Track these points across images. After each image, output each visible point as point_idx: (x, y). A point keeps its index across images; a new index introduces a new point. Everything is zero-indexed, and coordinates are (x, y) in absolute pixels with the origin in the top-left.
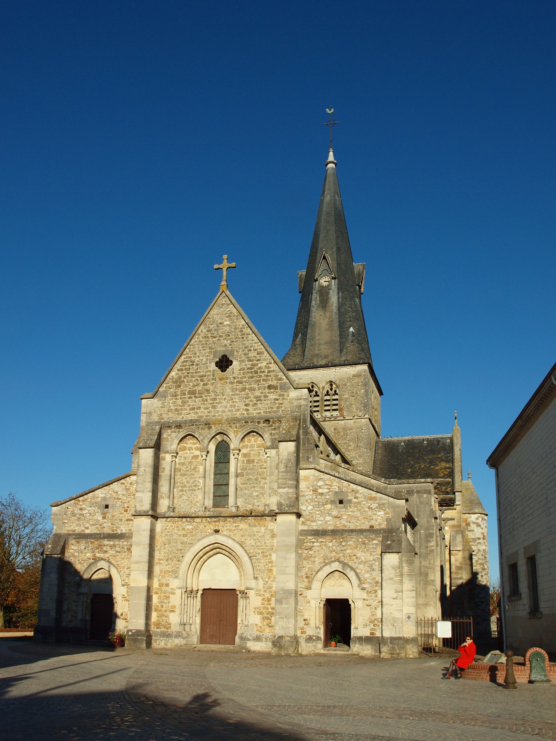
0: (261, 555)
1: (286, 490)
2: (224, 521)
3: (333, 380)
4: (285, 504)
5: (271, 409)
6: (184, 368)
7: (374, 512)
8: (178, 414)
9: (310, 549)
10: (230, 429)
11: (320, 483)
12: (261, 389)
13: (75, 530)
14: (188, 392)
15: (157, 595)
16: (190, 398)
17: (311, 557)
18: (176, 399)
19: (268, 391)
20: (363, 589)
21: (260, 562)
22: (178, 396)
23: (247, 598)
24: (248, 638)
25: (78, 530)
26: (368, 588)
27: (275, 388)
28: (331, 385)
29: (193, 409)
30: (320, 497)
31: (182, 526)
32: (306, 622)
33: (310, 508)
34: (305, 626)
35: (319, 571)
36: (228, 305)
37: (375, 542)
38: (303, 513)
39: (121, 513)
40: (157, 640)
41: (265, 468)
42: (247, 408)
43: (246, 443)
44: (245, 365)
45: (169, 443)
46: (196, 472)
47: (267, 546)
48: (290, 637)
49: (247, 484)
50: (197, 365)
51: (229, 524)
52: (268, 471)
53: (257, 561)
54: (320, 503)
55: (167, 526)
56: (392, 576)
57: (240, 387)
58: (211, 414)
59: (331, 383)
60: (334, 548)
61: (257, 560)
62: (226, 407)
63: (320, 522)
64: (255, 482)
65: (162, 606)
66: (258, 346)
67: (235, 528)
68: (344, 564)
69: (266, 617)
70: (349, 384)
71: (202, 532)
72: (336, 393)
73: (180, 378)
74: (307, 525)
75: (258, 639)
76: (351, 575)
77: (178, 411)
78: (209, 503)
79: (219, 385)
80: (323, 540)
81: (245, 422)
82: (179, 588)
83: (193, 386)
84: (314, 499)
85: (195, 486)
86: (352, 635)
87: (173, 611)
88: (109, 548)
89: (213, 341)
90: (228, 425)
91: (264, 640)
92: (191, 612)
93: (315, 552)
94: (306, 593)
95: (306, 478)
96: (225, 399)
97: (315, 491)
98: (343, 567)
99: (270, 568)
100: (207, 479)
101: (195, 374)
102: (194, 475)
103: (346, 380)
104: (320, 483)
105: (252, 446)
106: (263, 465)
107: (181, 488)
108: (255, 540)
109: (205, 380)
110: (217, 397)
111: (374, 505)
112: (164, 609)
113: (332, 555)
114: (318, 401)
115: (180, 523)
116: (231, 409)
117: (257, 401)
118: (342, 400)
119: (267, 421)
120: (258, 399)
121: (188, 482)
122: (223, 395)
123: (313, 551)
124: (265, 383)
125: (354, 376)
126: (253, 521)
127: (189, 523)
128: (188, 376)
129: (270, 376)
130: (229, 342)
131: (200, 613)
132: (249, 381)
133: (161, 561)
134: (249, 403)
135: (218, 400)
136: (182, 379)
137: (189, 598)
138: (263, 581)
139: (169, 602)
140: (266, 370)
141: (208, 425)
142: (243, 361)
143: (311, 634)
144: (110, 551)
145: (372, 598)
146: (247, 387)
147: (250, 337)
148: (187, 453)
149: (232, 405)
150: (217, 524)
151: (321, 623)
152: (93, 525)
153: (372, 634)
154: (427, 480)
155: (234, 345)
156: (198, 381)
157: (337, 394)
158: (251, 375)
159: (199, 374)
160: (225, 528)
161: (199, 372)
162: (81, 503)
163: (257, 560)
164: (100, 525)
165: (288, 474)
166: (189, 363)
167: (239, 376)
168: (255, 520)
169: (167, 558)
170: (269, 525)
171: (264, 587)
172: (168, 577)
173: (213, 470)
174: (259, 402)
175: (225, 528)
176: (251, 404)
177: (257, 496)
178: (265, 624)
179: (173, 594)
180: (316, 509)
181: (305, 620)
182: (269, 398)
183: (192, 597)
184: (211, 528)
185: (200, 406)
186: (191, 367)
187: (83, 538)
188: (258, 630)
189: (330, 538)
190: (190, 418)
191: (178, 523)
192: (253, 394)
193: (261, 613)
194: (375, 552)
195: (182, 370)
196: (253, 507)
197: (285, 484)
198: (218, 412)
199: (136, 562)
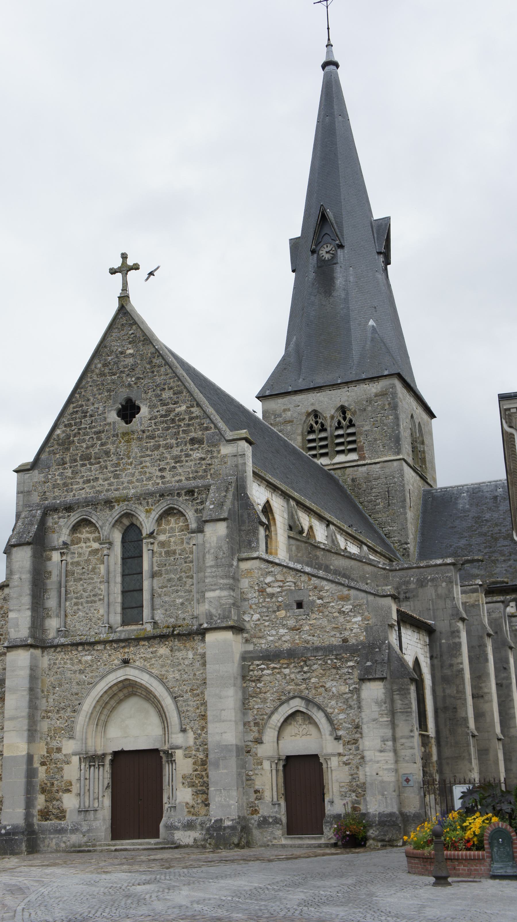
0: (190, 693)
1: (217, 593)
2: (136, 646)
3: (346, 404)
4: (217, 615)
5: (195, 474)
6: (73, 422)
7: (348, 618)
8: (67, 491)
9: (259, 680)
10: (140, 507)
11: (269, 579)
12: (181, 445)
14: (80, 457)
15: (45, 767)
16: (83, 465)
17: (260, 693)
18: (64, 469)
19: (190, 447)
20: (338, 738)
21: (188, 705)
22: (66, 463)
23: (173, 762)
24: (175, 826)
26: (345, 737)
27: (200, 442)
28: (344, 413)
29: (88, 481)
30: (269, 600)
31: (77, 658)
32: (258, 794)
33: (256, 617)
34: (256, 802)
35: (272, 713)
37: (351, 664)
38: (248, 626)
40: (45, 838)
41: (192, 562)
42: (163, 474)
43: (164, 526)
44: (157, 412)
45: (55, 536)
46: (95, 574)
47: (198, 679)
48: (232, 820)
49: (167, 587)
50: (91, 416)
51: (142, 650)
52: (195, 566)
53: (184, 704)
54: (270, 609)
55: (57, 659)
56: (376, 715)
57: (152, 444)
58: (112, 488)
59: (343, 410)
60: (293, 676)
61: (184, 701)
62: (133, 475)
63: (271, 638)
64: (178, 582)
65: (52, 784)
66: (174, 381)
67: (152, 655)
68: (308, 701)
69: (199, 791)
70: (370, 408)
71: (105, 665)
72: (351, 424)
73: (68, 437)
74: (253, 642)
75: (189, 826)
76: (319, 717)
77: (67, 486)
78: (116, 618)
80: (276, 666)
81: (160, 496)
82: (75, 754)
83: (87, 448)
84: (261, 603)
85: (94, 595)
86: (327, 812)
87: (68, 791)
89: (112, 380)
90: (136, 502)
91: (199, 827)
92: (96, 791)
93: (265, 684)
94: (256, 748)
95: (249, 571)
96: (131, 463)
97: (262, 591)
98: (307, 705)
99: (203, 713)
100: (112, 584)
101: (88, 430)
102: (92, 579)
103: (365, 403)
104: (269, 579)
105: (172, 530)
106: (188, 557)
107: (74, 600)
108: (179, 671)
109: (103, 437)
110: (121, 462)
111: (347, 607)
112: (55, 788)
113: (290, 687)
114: (325, 439)
115: (74, 652)
116: (140, 477)
117: (176, 462)
118: (361, 434)
120: (177, 460)
121: (85, 590)
122: (129, 458)
123: (263, 683)
124: (185, 435)
125: (376, 395)
126: (177, 643)
127: (87, 653)
128: (79, 433)
129: (193, 425)
130: (133, 379)
131: (110, 790)
132: (163, 434)
133: (50, 714)
134: (166, 467)
135: (122, 465)
136: (71, 438)
137: (92, 768)
138: (194, 733)
139: (62, 777)
140: (187, 417)
141: (109, 503)
142: (155, 406)
143: (266, 814)
145: (351, 751)
146: (161, 443)
147: (163, 369)
148: (82, 548)
149: (141, 472)
150: (127, 650)
151: (281, 796)
153: (354, 809)
154: (445, 560)
155: (142, 383)
156: (93, 440)
158: (166, 425)
159: (94, 429)
160: (138, 656)
161: (94, 427)
163: (184, 701)
165: (220, 569)
166: (80, 415)
167: (150, 428)
168: (179, 640)
169: (57, 708)
170: (199, 648)
171: (195, 743)
172: (59, 737)
173: (119, 569)
174: (178, 464)
175: (138, 656)
176: (168, 469)
177: (182, 604)
178: (199, 801)
179: (68, 763)
180: (264, 618)
181: (256, 792)
182: (192, 458)
183: (97, 766)
185: (97, 476)
186: (83, 421)
188: (189, 812)
189: (286, 661)
190: (83, 496)
191: (71, 653)
192: (169, 453)
193: (192, 785)
194: (352, 679)
195: (70, 425)
196: (177, 620)
197: (215, 585)
198: (123, 483)
199: (12, 719)
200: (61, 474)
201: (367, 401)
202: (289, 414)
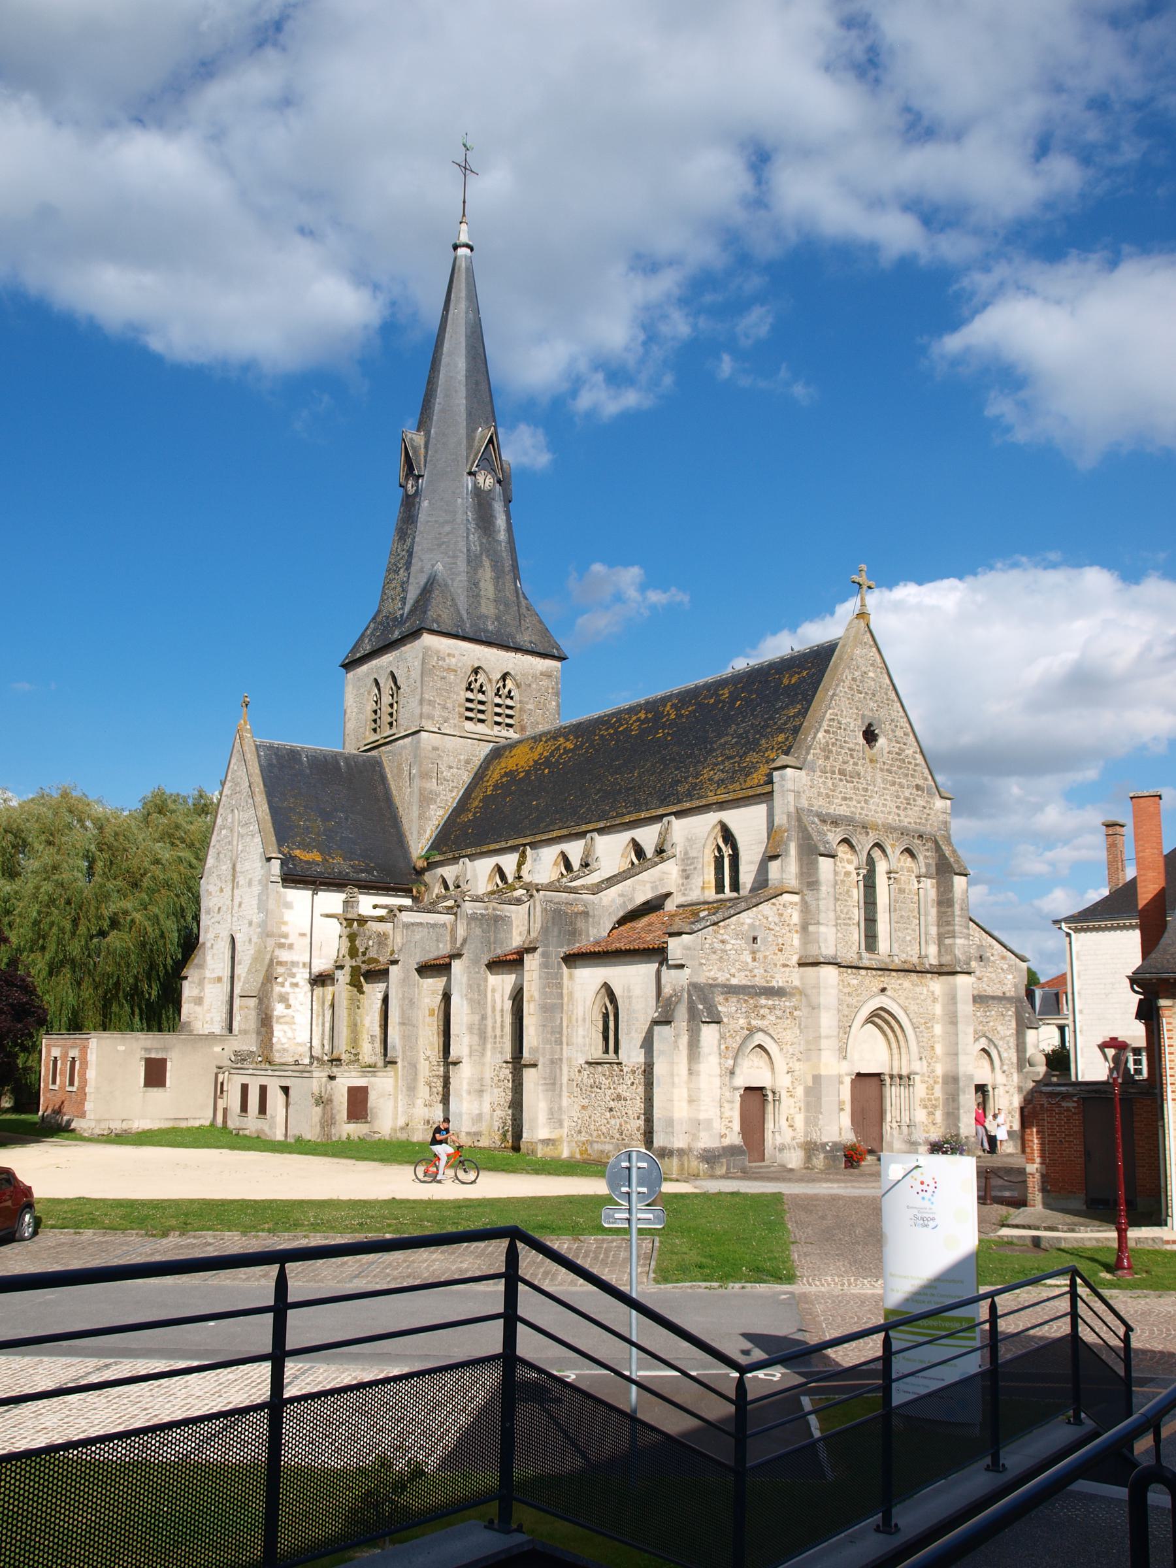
3: (512, 673)
13: (717, 978)
16: (841, 780)
18: (826, 778)
25: (722, 978)
29: (845, 799)
36: (871, 646)
39: (775, 954)
79: (869, 769)
85: (849, 919)
88: (767, 1011)
102: (846, 900)
119: (921, 836)
144: (769, 1017)
152: (740, 970)
157: (512, 698)
162: (722, 931)
164: (751, 971)
184: (876, 985)
187: (734, 993)
199: (827, 1037)
200: (824, 783)
202: (453, 660)
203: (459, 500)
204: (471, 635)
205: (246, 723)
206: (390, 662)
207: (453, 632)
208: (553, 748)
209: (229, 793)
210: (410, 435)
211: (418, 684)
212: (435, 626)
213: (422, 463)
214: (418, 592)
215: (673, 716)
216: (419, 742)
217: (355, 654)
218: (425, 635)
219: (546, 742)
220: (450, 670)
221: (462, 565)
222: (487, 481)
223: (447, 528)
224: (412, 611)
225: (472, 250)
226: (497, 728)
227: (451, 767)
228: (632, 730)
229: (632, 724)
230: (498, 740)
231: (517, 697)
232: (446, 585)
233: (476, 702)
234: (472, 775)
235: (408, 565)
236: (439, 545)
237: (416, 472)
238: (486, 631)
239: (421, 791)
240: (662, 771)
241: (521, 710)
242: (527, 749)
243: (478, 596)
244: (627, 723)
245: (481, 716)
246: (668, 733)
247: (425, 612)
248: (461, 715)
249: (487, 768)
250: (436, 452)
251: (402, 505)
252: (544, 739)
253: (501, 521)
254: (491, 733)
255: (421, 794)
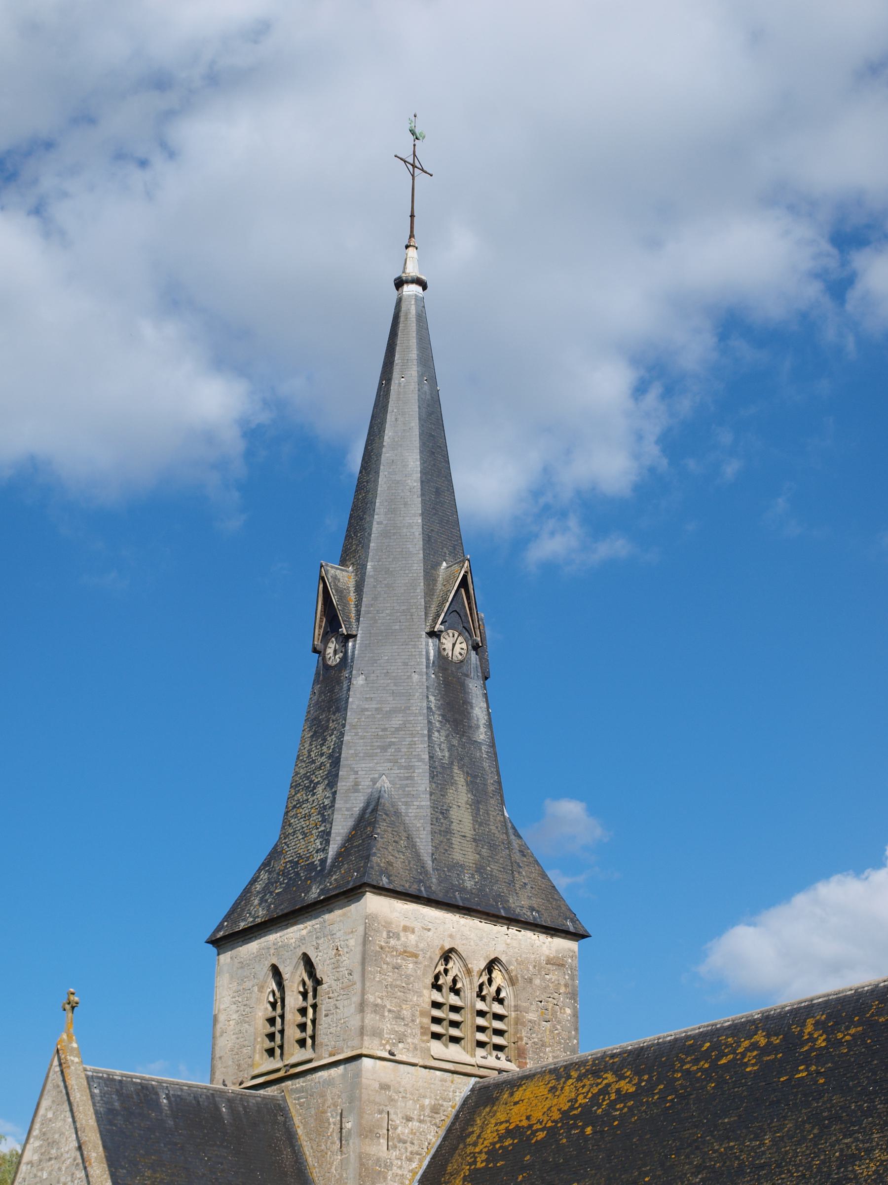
3: (503, 959)
103: (531, 968)
157: (501, 1001)
201: (535, 967)
202: (412, 938)
203: (416, 677)
204: (440, 897)
205: (70, 1042)
206: (302, 939)
207: (413, 890)
208: (595, 1090)
209: (36, 1158)
210: (332, 572)
211: (357, 977)
212: (384, 881)
213: (353, 615)
214: (350, 823)
215: (821, 1043)
216: (358, 1074)
217: (236, 922)
218: (369, 895)
219: (579, 1079)
220: (409, 954)
221: (422, 783)
222: (458, 646)
223: (396, 721)
224: (343, 854)
225: (424, 286)
226: (480, 1052)
227: (409, 1119)
228: (746, 1065)
229: (743, 1055)
230: (482, 1072)
231: (510, 1001)
232: (397, 814)
233: (446, 1008)
234: (442, 1133)
235: (332, 780)
236: (384, 749)
237: (344, 630)
238: (463, 890)
239: (362, 1158)
240: (818, 1137)
241: (517, 1021)
242: (543, 1090)
243: (448, 832)
244: (734, 1052)
245: (454, 1032)
246: (818, 1073)
247: (367, 858)
248: (424, 1030)
249: (470, 1121)
250: (375, 598)
251: (316, 681)
252: (574, 1074)
253: (479, 711)
254: (472, 1061)
255: (362, 1164)
